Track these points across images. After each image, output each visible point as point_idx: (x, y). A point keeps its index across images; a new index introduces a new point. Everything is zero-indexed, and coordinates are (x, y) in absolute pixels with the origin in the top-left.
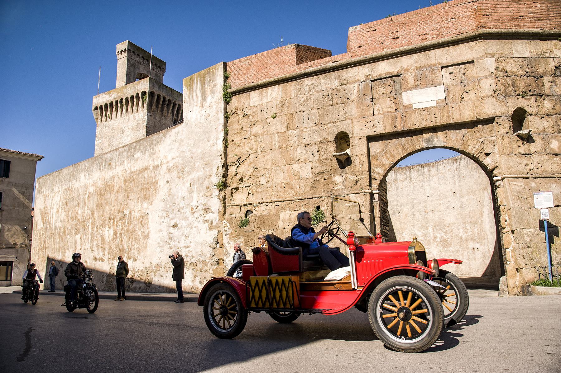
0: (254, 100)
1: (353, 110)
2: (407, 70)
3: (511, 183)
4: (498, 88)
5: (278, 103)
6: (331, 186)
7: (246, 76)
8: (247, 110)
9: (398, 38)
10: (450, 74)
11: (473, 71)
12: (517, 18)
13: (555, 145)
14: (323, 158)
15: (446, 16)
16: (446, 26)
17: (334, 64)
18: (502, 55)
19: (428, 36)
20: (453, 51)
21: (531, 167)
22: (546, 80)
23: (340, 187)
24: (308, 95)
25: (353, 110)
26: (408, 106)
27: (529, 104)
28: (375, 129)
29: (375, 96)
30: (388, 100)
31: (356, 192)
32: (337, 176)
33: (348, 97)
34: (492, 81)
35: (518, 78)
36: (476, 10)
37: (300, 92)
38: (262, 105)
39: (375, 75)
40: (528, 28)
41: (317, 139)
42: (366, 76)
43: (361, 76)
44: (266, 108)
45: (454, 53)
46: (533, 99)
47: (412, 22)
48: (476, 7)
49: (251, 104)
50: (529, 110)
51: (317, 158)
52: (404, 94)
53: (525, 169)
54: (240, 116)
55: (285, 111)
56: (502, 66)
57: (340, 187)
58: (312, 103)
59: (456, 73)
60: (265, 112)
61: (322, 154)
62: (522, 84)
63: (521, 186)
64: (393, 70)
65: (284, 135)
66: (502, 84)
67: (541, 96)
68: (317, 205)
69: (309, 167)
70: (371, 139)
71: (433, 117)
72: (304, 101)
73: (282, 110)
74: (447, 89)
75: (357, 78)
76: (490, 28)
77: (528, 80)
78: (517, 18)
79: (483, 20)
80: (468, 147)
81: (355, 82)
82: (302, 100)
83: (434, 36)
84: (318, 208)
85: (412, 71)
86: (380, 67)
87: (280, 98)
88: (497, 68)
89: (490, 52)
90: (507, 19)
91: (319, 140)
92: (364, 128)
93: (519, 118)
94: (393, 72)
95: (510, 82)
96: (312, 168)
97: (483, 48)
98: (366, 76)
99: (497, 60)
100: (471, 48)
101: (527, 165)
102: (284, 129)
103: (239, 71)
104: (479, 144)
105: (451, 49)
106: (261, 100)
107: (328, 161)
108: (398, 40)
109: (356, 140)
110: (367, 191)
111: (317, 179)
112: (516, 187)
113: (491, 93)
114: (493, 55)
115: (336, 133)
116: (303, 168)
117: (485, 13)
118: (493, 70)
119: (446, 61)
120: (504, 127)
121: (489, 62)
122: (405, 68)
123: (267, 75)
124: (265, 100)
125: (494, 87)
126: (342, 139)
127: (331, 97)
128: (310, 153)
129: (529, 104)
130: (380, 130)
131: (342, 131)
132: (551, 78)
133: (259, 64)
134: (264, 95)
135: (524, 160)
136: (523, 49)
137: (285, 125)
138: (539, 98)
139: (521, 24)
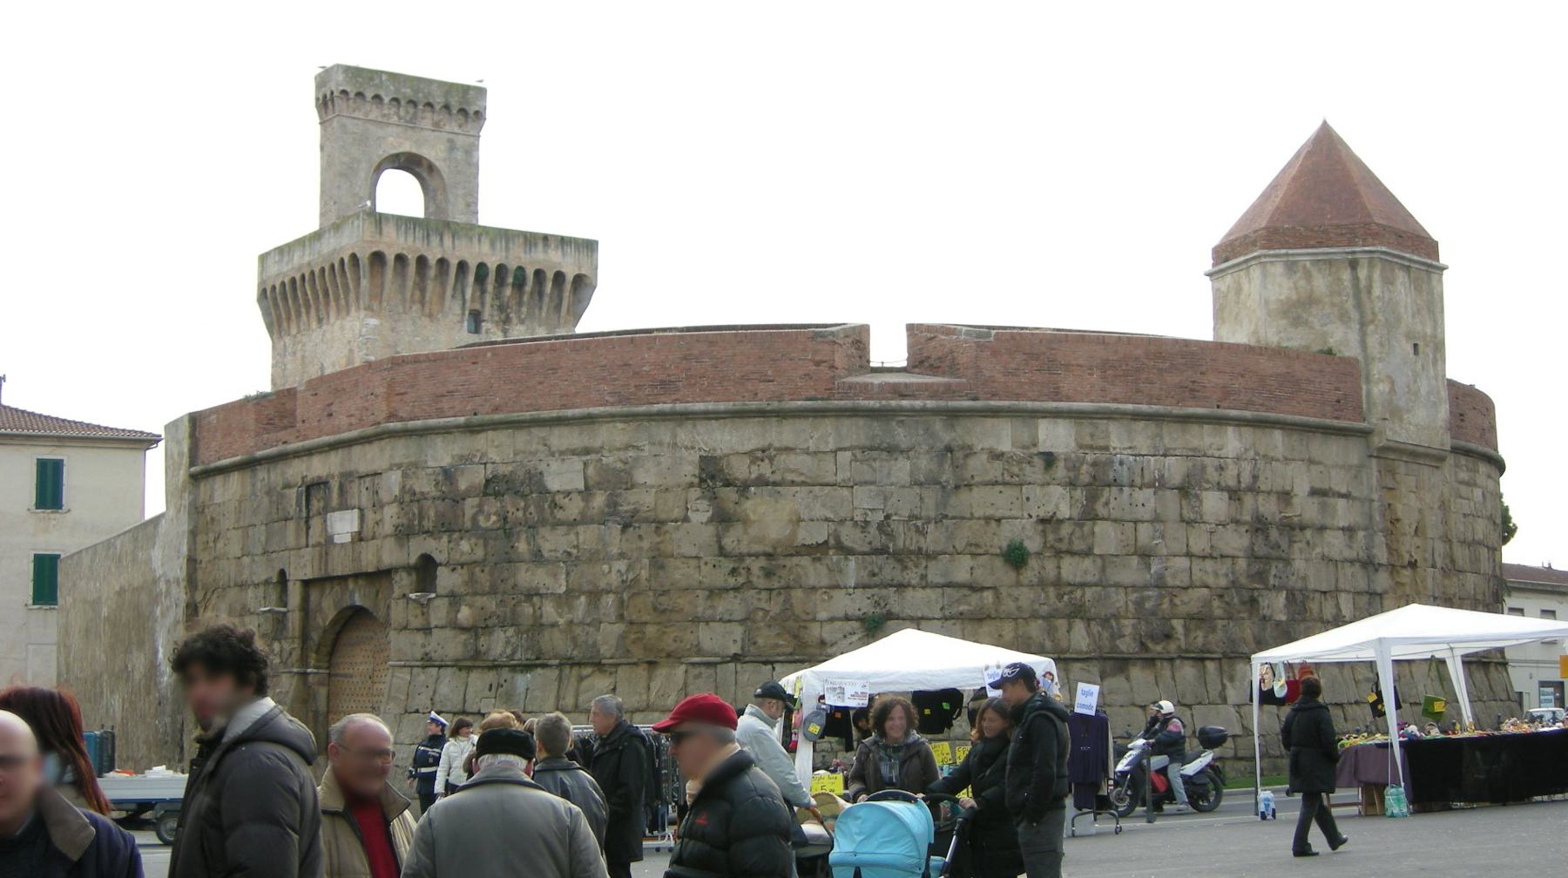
13: (465, 614)
21: (428, 649)
22: (470, 505)
27: (438, 548)
46: (445, 538)
50: (438, 558)
56: (409, 483)
62: (432, 513)
74: (362, 518)
89: (397, 460)
93: (426, 569)
99: (405, 475)
101: (424, 646)
118: (397, 491)
125: (395, 521)
130: (309, 576)
132: (476, 501)
135: (420, 638)
136: (441, 453)
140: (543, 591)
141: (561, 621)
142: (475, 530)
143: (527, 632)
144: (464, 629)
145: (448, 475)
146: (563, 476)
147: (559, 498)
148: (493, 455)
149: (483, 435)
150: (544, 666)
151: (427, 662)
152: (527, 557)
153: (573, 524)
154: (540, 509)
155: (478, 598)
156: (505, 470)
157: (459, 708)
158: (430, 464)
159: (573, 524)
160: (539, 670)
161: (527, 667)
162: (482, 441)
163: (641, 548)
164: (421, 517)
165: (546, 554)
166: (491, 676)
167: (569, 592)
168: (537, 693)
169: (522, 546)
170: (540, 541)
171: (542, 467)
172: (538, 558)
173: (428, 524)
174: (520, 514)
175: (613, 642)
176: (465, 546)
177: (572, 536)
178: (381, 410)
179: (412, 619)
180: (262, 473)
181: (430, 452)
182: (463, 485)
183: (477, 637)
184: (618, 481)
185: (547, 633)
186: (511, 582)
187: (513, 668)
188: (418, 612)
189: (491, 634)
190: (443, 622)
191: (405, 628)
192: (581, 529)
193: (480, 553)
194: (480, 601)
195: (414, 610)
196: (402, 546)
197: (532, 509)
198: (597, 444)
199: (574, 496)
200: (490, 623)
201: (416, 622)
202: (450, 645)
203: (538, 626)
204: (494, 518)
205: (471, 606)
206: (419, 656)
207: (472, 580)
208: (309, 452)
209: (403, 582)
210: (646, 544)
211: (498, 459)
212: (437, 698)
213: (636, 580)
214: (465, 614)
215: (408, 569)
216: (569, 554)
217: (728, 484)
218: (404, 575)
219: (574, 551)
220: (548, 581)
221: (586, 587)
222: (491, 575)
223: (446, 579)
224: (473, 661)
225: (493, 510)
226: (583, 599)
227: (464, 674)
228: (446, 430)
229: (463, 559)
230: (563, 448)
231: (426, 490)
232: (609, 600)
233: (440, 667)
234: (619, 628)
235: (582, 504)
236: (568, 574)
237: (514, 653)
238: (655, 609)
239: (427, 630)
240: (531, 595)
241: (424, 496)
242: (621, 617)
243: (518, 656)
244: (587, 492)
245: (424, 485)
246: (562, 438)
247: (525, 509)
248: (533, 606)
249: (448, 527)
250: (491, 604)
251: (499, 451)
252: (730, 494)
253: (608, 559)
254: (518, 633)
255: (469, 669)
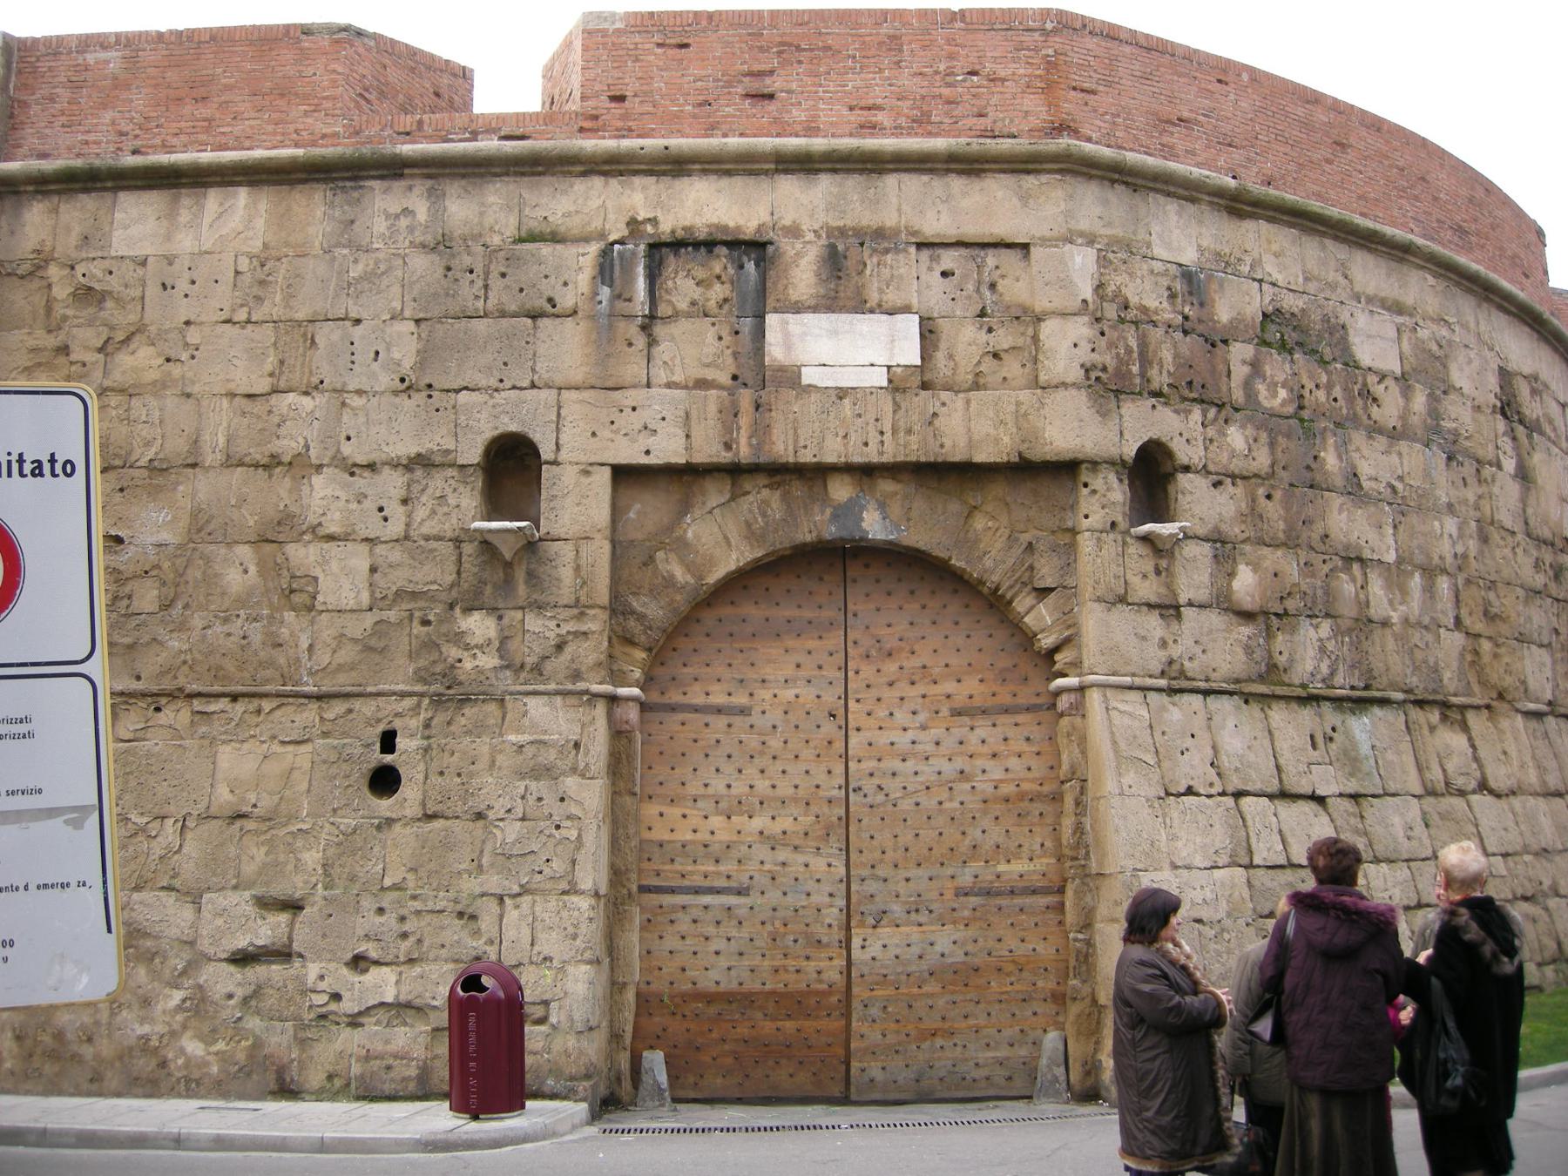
0: (135, 231)
1: (565, 349)
2: (794, 232)
3: (1113, 704)
4: (1096, 358)
5: (244, 265)
6: (453, 652)
7: (108, 116)
8: (96, 269)
9: (771, 97)
10: (944, 274)
11: (1019, 283)
12: (1169, 122)
13: (1245, 583)
14: (425, 530)
15: (951, 57)
16: (946, 91)
17: (510, 147)
18: (1115, 243)
19: (880, 117)
20: (965, 194)
21: (1175, 651)
22: (1240, 353)
23: (489, 661)
24: (381, 255)
25: (565, 349)
26: (782, 369)
27: (1182, 431)
28: (651, 442)
29: (664, 309)
30: (711, 334)
31: (552, 687)
32: (476, 615)
33: (549, 293)
34: (1080, 329)
35: (1160, 332)
36: (1051, 65)
37: (347, 236)
38: (170, 260)
39: (669, 224)
40: (1198, 165)
41: (406, 448)
42: (633, 223)
43: (611, 216)
44: (187, 276)
45: (965, 203)
47: (827, 48)
48: (1050, 52)
49: (119, 246)
50: (1184, 453)
51: (395, 528)
52: (772, 320)
53: (1155, 659)
54: (61, 292)
55: (273, 307)
56: (1116, 281)
57: (489, 661)
58: (396, 289)
59: (965, 277)
60: (178, 293)
61: (421, 513)
62: (1167, 355)
63: (1139, 718)
64: (742, 222)
65: (258, 407)
66: (1112, 345)
67: (1220, 406)
68: (381, 728)
69: (359, 559)
70: (624, 475)
71: (871, 428)
72: (368, 277)
73: (258, 299)
74: (928, 333)
75: (596, 224)
76: (1089, 140)
77: (1188, 345)
78: (1169, 122)
79: (1070, 105)
80: (980, 558)
81: (586, 239)
82: (356, 271)
83: (903, 121)
84: (388, 742)
85: (810, 236)
86: (693, 195)
87: (256, 245)
88: (1100, 287)
89: (1084, 225)
90: (1140, 121)
91: (413, 450)
92: (605, 433)
93: (1151, 475)
94: (738, 228)
95: (1133, 343)
96: (373, 570)
97: (1063, 206)
98: (633, 223)
99: (1103, 261)
100: (1025, 198)
101: (1163, 644)
102: (263, 385)
103: (74, 86)
104: (1017, 551)
105: (956, 183)
106: (168, 238)
107: (446, 548)
108: (772, 107)
109: (568, 475)
110: (596, 688)
111: (392, 615)
112: (1127, 721)
113: (1076, 374)
114: (1091, 240)
115: (489, 434)
116: (335, 566)
117: (1077, 79)
118: (1087, 293)
119: (936, 224)
120: (1104, 501)
121: (1078, 259)
122: (787, 222)
123: (207, 130)
124: (185, 243)
125: (1084, 354)
126: (512, 466)
127: (480, 283)
128: (370, 505)
129: (1182, 431)
130: (668, 449)
131: (513, 427)
133: (171, 75)
134: (184, 216)
135: (1153, 624)
136: (1180, 237)
137: (269, 368)
138: (1212, 412)
139: (1180, 147)
140: (1367, 554)
141: (1395, 617)
142: (1247, 410)
143: (1350, 631)
144: (1247, 616)
145: (1192, 284)
146: (1375, 345)
147: (1372, 379)
148: (1271, 269)
149: (1249, 225)
150: (1384, 702)
151: (1176, 683)
152: (1339, 482)
153: (1394, 435)
154: (1350, 400)
155: (1266, 551)
156: (1292, 303)
157: (1274, 787)
158: (1158, 251)
159: (1394, 435)
160: (1377, 711)
161: (1360, 704)
162: (1255, 236)
163: (1465, 502)
164: (1145, 362)
165: (1366, 484)
166: (1306, 714)
167: (1400, 561)
168: (1390, 756)
169: (1330, 460)
170: (1355, 455)
171: (1344, 317)
172: (1353, 487)
173: (1160, 379)
174: (1321, 395)
175: (1455, 665)
176: (1236, 437)
177: (1395, 458)
178: (1035, 109)
179: (1135, 580)
180: (384, 204)
181: (1156, 228)
182: (1224, 313)
183: (1269, 635)
184: (1426, 371)
185: (1377, 633)
186: (1319, 528)
187: (1338, 701)
188: (1149, 566)
189: (1293, 630)
190: (1202, 595)
191: (1122, 600)
192: (1403, 445)
193: (1262, 461)
194: (1273, 558)
195: (1139, 560)
196: (1104, 414)
197: (1337, 391)
198: (1409, 300)
199: (1389, 382)
200: (1291, 604)
201: (1147, 589)
202: (1219, 647)
203: (1365, 624)
204: (1283, 393)
205: (1256, 566)
206: (1156, 667)
207: (1253, 514)
208: (676, 166)
209: (1106, 497)
210: (1470, 495)
211: (1279, 277)
212: (1225, 761)
213: (1465, 556)
214: (1245, 583)
215: (1117, 464)
216: (1393, 488)
217: (1521, 422)
218: (1112, 477)
219: (1399, 486)
220: (1371, 535)
221: (1419, 558)
222: (1287, 505)
223: (1199, 504)
224: (1264, 687)
225: (1281, 378)
226: (1417, 575)
227: (1255, 709)
228: (1187, 191)
229: (1236, 466)
230: (1370, 291)
231: (1152, 303)
232: (1443, 584)
233: (1206, 693)
234: (1458, 639)
235: (1401, 401)
236: (1395, 527)
237: (1332, 674)
238: (1486, 613)
239: (1170, 609)
240: (1353, 559)
241: (1146, 319)
242: (1458, 621)
243: (1339, 680)
244: (1404, 380)
245: (1146, 292)
246: (1369, 273)
247: (1329, 387)
248: (1354, 580)
249: (1198, 392)
250: (1289, 566)
251: (1280, 265)
252: (1520, 430)
253: (1436, 511)
254: (1337, 632)
255: (1266, 699)
